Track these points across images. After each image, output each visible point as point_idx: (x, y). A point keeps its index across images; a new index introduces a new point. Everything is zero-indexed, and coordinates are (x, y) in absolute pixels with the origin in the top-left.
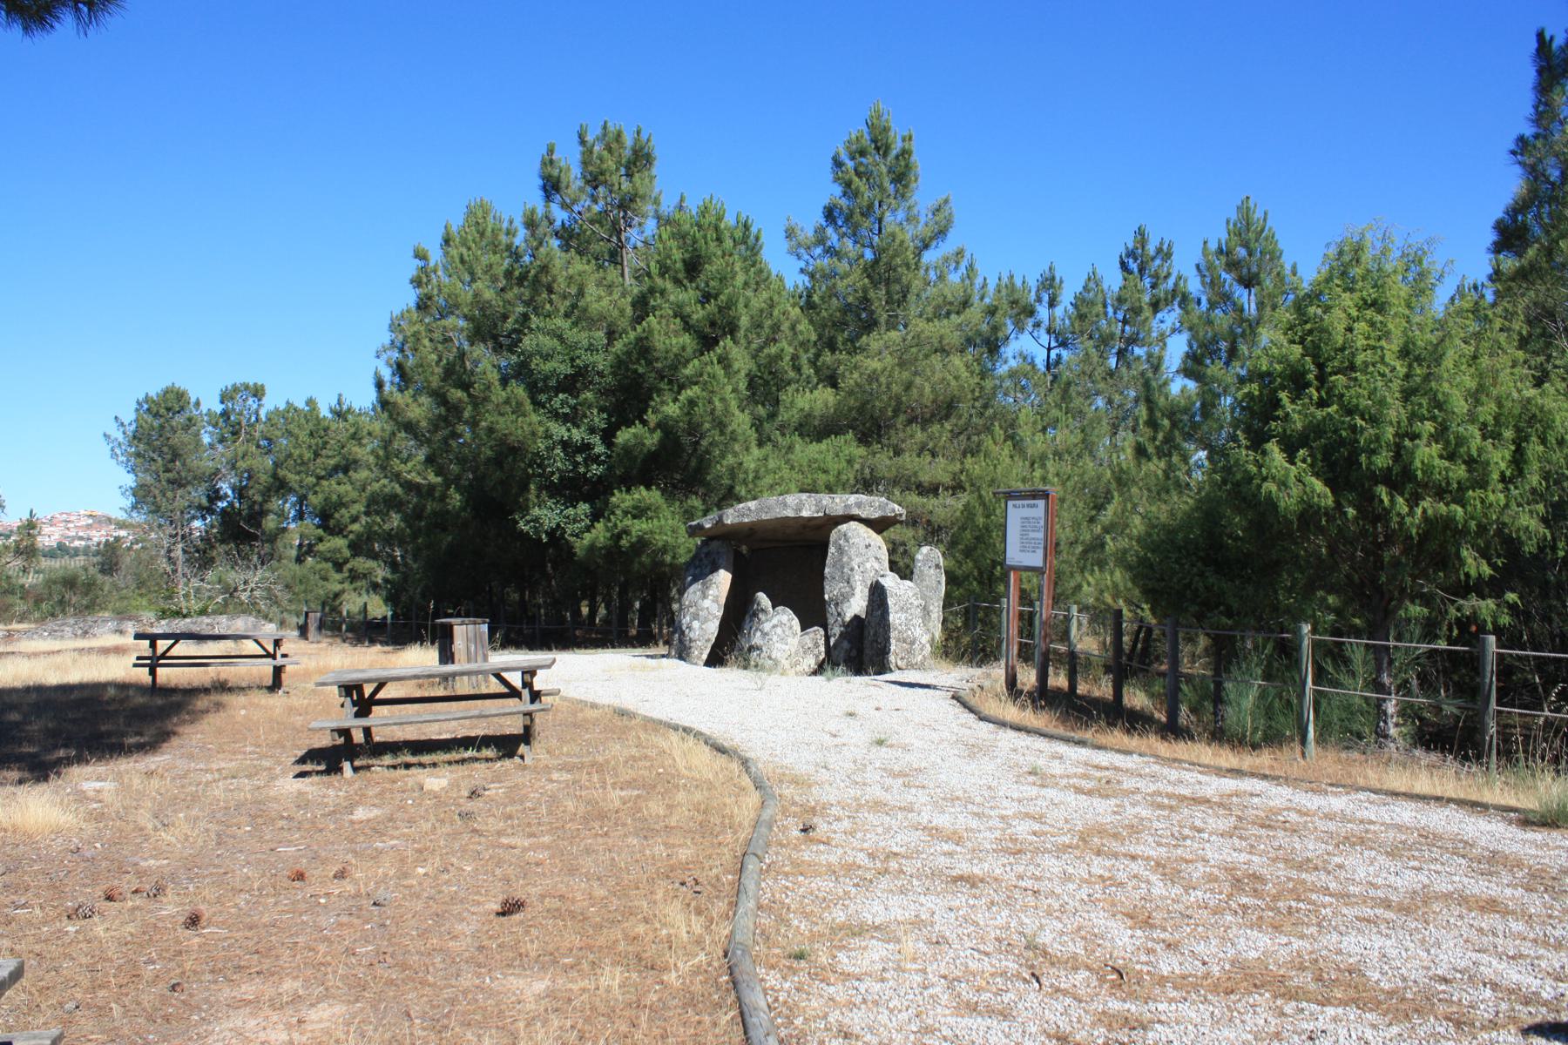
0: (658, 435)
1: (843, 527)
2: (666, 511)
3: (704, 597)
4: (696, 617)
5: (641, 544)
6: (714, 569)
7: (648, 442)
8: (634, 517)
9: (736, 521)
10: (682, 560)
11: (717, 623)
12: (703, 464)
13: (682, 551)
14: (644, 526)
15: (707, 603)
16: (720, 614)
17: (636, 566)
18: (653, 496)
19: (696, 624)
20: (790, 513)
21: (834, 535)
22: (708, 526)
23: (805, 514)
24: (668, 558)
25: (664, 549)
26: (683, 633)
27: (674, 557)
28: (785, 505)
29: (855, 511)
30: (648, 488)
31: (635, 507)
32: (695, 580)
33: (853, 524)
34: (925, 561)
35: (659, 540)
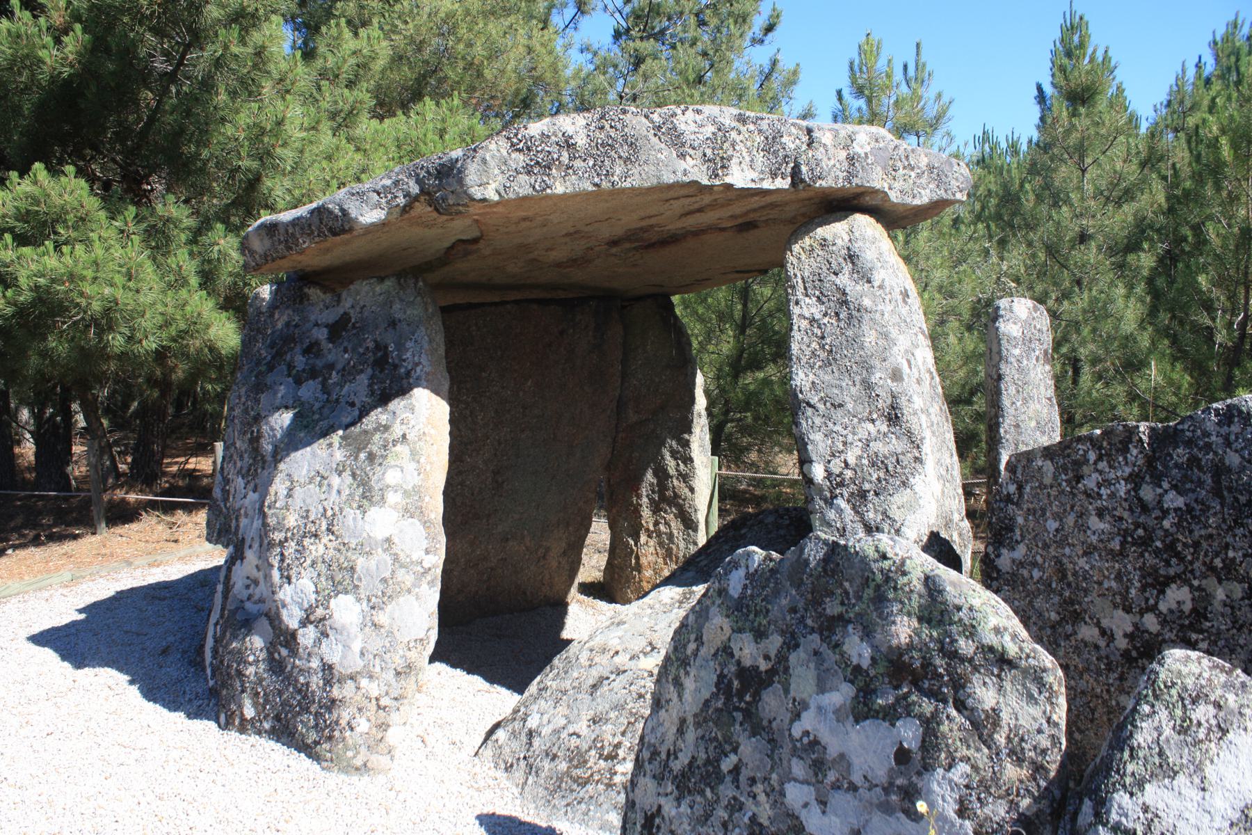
0: (75, 42)
1: (836, 231)
2: (104, 229)
3: (367, 495)
4: (340, 578)
5: (45, 309)
6: (391, 387)
7: (48, 55)
8: (22, 240)
9: (523, 186)
10: (151, 344)
11: (431, 596)
12: (196, 115)
13: (147, 322)
14: (51, 262)
15: (381, 522)
16: (437, 560)
17: (34, 360)
18: (67, 190)
19: (345, 610)
20: (694, 170)
21: (802, 259)
22: (369, 215)
23: (740, 177)
24: (116, 341)
25: (106, 321)
26: (289, 639)
27: (130, 339)
28: (676, 140)
29: (876, 179)
30: (54, 171)
31: (24, 216)
32: (309, 428)
33: (863, 224)
34: (1027, 341)
35: (95, 296)
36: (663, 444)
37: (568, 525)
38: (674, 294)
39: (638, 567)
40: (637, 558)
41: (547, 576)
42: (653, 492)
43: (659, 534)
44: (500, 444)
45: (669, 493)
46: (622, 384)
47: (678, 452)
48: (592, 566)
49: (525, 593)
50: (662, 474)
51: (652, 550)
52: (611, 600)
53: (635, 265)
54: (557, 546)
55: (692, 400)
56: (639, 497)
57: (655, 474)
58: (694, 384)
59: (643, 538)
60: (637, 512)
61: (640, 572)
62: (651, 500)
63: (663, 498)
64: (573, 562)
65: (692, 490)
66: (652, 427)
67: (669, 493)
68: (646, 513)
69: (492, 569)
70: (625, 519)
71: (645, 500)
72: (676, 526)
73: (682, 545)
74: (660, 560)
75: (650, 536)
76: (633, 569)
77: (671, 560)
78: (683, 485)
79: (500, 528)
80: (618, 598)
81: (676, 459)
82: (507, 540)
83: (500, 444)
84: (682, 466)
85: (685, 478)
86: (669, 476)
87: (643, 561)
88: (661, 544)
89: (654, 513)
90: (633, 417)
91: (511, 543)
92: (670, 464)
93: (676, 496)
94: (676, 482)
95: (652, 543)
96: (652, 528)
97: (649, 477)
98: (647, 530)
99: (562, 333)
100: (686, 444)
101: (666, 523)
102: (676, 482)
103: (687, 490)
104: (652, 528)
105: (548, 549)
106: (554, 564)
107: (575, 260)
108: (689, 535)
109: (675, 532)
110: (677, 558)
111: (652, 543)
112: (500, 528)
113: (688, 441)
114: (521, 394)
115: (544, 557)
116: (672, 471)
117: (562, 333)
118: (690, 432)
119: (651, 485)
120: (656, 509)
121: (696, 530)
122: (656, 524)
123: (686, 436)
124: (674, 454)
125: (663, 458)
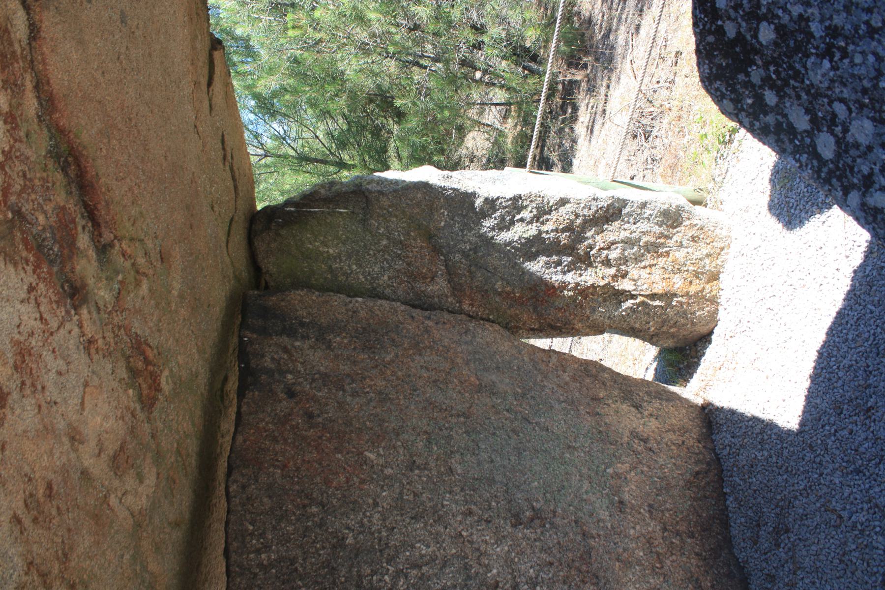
36: (488, 242)
37: (595, 399)
38: (255, 206)
39: (667, 296)
40: (653, 296)
41: (671, 436)
42: (559, 263)
43: (624, 260)
44: (470, 513)
45: (564, 238)
46: (387, 298)
47: (502, 218)
48: (631, 358)
49: (698, 473)
50: (534, 247)
51: (644, 273)
52: (706, 338)
53: (163, 258)
54: (626, 420)
55: (424, 187)
56: (564, 286)
57: (533, 257)
58: (396, 182)
59: (625, 285)
60: (584, 292)
61: (675, 295)
62: (571, 267)
63: (570, 249)
64: (648, 394)
65: (563, 202)
66: (458, 257)
67: (564, 238)
68: (591, 277)
69: (665, 529)
70: (594, 310)
71: (571, 278)
72: (614, 232)
73: (643, 226)
74: (662, 261)
75: (624, 276)
76: (669, 305)
77: (662, 245)
78: (554, 216)
79: (604, 515)
80: (704, 330)
81: (512, 223)
82: (621, 502)
83: (470, 513)
84: (526, 214)
85: (543, 212)
86: (538, 238)
87: (659, 289)
88: (637, 259)
89: (590, 265)
90: (439, 286)
91: (626, 497)
92: (519, 232)
93: (569, 228)
94: (549, 226)
95: (634, 272)
96: (613, 271)
97: (536, 267)
98: (615, 277)
99: (291, 394)
100: (491, 204)
101: (608, 248)
102: (549, 226)
103: (562, 210)
104: (613, 271)
105: (634, 434)
106: (653, 424)
107: (134, 373)
108: (630, 214)
109: (624, 235)
110: (661, 235)
111: (634, 272)
112: (604, 515)
113: (486, 199)
114: (388, 471)
115: (645, 441)
116: (532, 231)
117: (291, 394)
118: (474, 195)
119: (548, 265)
120: (585, 261)
121: (624, 203)
122: (607, 263)
123: (479, 202)
124: (505, 225)
125: (510, 244)
